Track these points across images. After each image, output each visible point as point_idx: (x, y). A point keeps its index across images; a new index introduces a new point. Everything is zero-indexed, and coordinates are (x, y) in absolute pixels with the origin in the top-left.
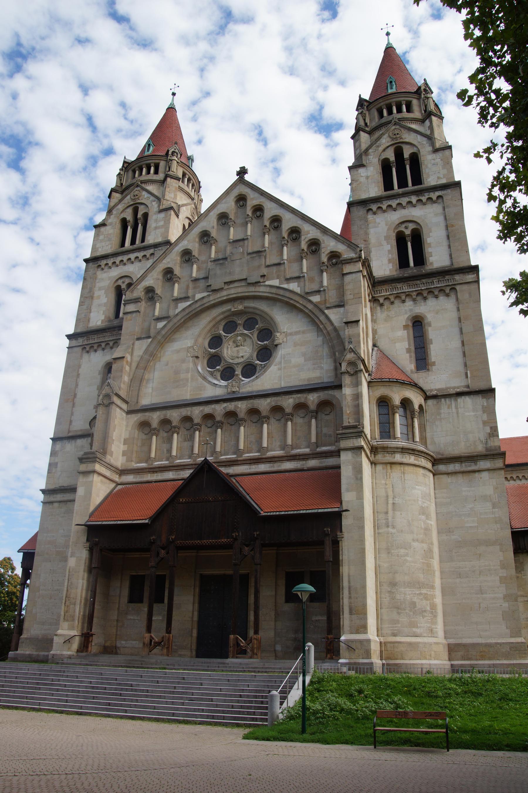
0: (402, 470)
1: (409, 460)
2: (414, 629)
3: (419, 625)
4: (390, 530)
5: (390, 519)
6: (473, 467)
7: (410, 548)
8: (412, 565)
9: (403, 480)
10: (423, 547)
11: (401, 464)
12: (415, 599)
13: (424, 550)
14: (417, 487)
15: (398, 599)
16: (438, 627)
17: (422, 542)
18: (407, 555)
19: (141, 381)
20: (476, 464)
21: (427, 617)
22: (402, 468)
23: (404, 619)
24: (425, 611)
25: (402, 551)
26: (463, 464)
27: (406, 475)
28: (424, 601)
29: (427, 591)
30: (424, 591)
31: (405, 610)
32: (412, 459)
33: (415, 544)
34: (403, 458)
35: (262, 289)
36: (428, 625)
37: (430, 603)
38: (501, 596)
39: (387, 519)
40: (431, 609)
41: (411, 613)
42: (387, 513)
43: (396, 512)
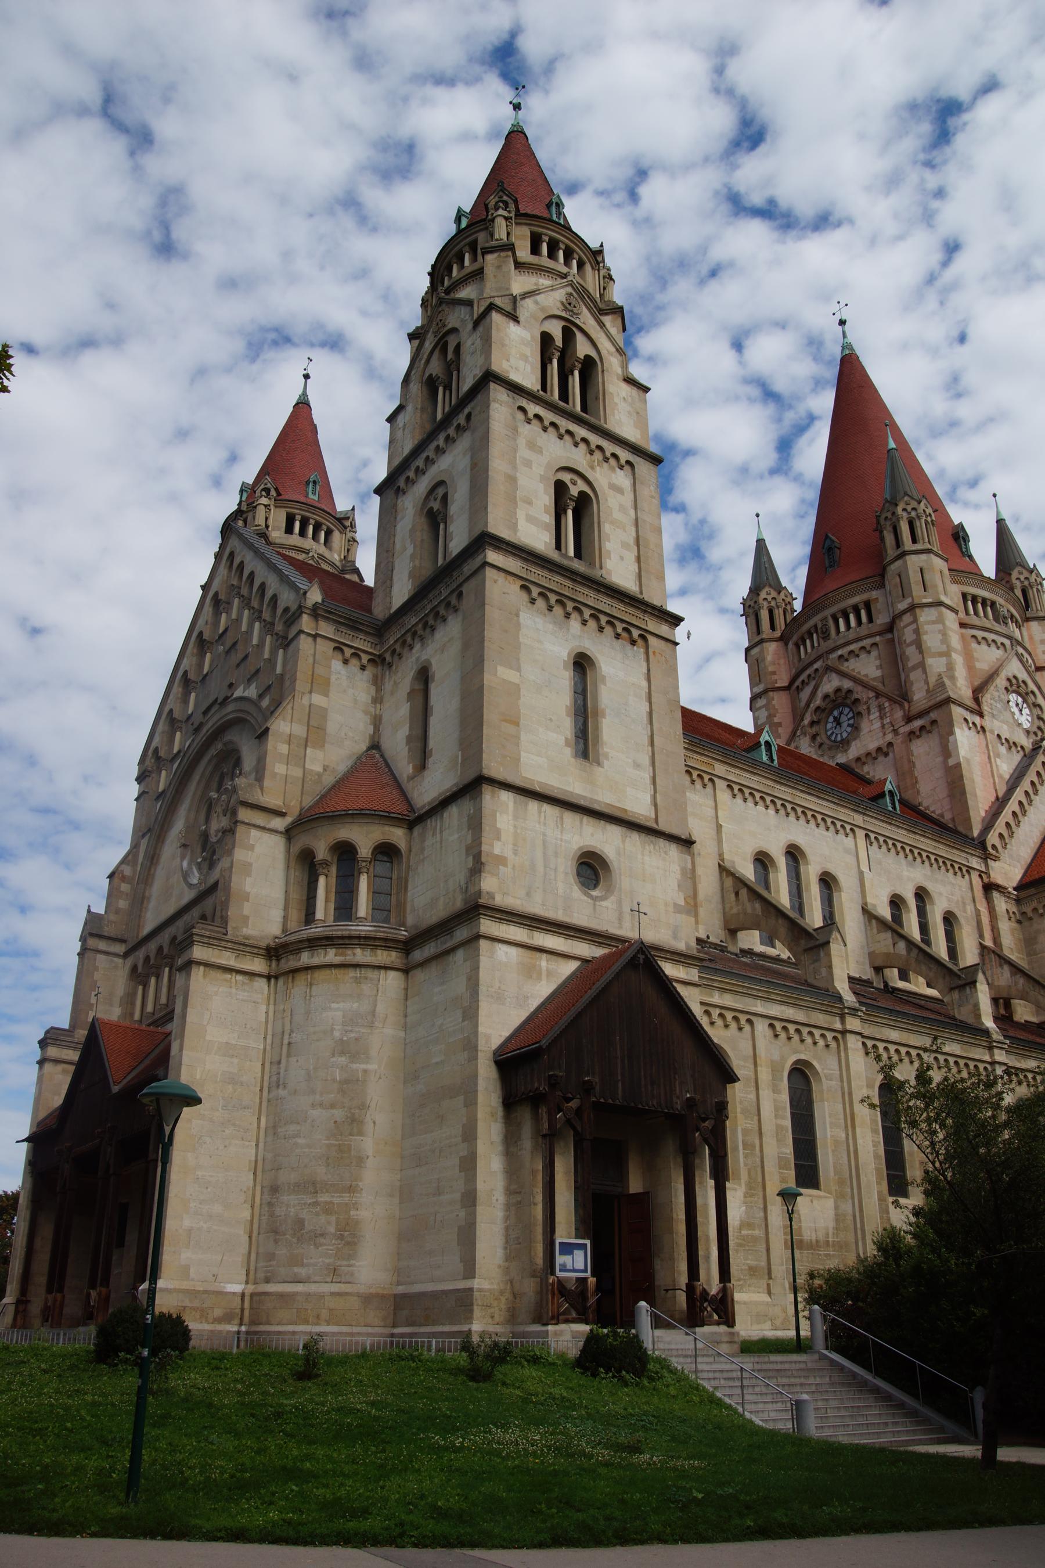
0: (309, 980)
1: (324, 957)
2: (296, 1269)
3: (305, 1261)
4: (282, 1092)
5: (282, 1071)
6: (449, 944)
7: (305, 1122)
8: (304, 1152)
9: (308, 998)
10: (333, 1115)
11: (308, 968)
12: (304, 1215)
13: (335, 1122)
14: (334, 1005)
15: (278, 1216)
16: (357, 1264)
17: (333, 1106)
18: (297, 1135)
19: (142, 902)
20: (452, 936)
21: (325, 1245)
22: (309, 977)
23: (282, 1252)
24: (322, 1235)
25: (293, 1128)
26: (439, 941)
27: (314, 988)
28: (323, 1218)
29: (333, 1197)
30: (324, 1198)
31: (284, 1235)
32: (331, 956)
33: (315, 1113)
34: (312, 957)
35: (230, 708)
36: (327, 1261)
37: (337, 1218)
38: (457, 1196)
39: (279, 1073)
40: (337, 1230)
41: (295, 1240)
42: (279, 1062)
43: (290, 1059)
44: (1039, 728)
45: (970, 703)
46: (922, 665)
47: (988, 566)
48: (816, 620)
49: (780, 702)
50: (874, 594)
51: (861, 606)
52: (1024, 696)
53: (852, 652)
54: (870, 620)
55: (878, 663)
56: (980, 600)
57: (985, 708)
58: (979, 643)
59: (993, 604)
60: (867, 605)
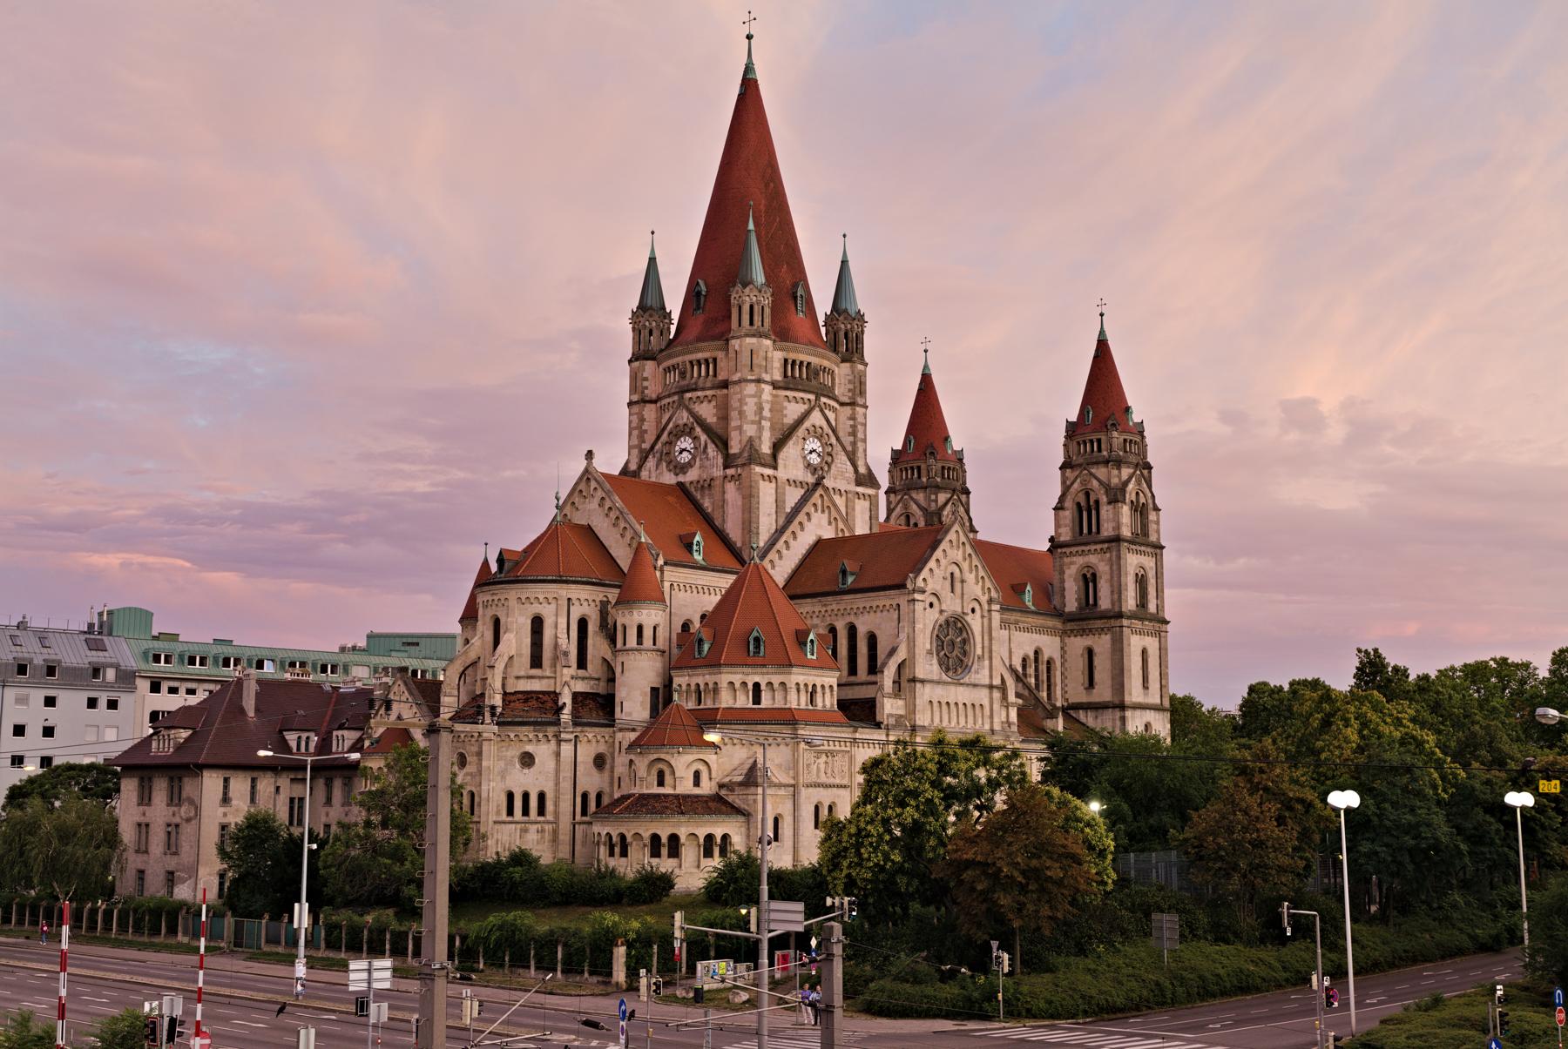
44: (826, 463)
45: (769, 460)
46: (740, 428)
47: (823, 306)
48: (679, 360)
50: (720, 355)
51: (710, 360)
52: (820, 438)
53: (698, 397)
54: (715, 375)
55: (715, 411)
56: (798, 362)
57: (780, 462)
58: (789, 401)
59: (809, 364)
60: (715, 360)
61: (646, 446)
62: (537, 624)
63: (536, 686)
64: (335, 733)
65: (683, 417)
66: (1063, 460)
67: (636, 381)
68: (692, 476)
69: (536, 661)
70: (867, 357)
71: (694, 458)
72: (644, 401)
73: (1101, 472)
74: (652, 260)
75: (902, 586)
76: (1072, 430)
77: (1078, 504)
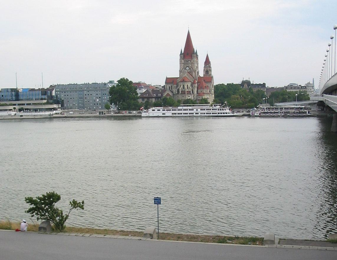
49: (183, 64)
61: (183, 67)
62: (187, 85)
63: (188, 90)
64: (159, 94)
65: (188, 65)
66: (204, 66)
67: (181, 61)
68: (189, 71)
69: (187, 88)
70: (199, 59)
71: (189, 69)
72: (182, 63)
73: (208, 68)
74: (181, 50)
75: (211, 82)
76: (205, 63)
77: (206, 71)
